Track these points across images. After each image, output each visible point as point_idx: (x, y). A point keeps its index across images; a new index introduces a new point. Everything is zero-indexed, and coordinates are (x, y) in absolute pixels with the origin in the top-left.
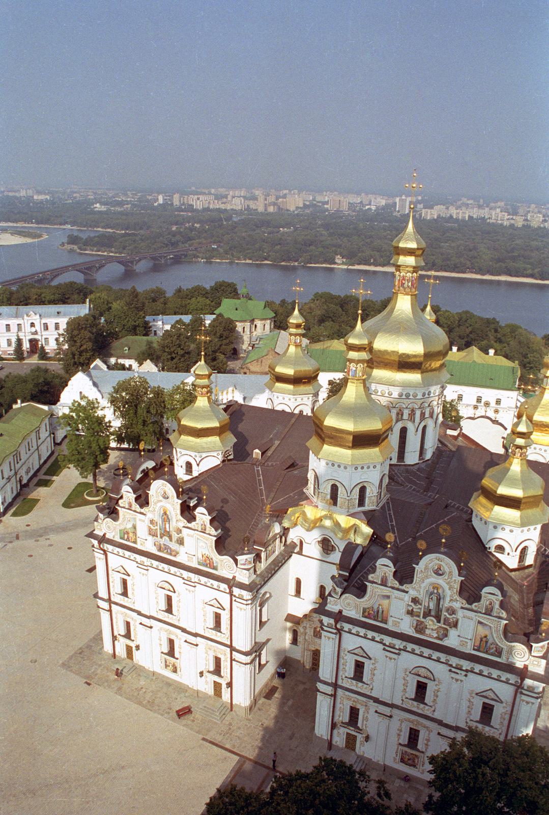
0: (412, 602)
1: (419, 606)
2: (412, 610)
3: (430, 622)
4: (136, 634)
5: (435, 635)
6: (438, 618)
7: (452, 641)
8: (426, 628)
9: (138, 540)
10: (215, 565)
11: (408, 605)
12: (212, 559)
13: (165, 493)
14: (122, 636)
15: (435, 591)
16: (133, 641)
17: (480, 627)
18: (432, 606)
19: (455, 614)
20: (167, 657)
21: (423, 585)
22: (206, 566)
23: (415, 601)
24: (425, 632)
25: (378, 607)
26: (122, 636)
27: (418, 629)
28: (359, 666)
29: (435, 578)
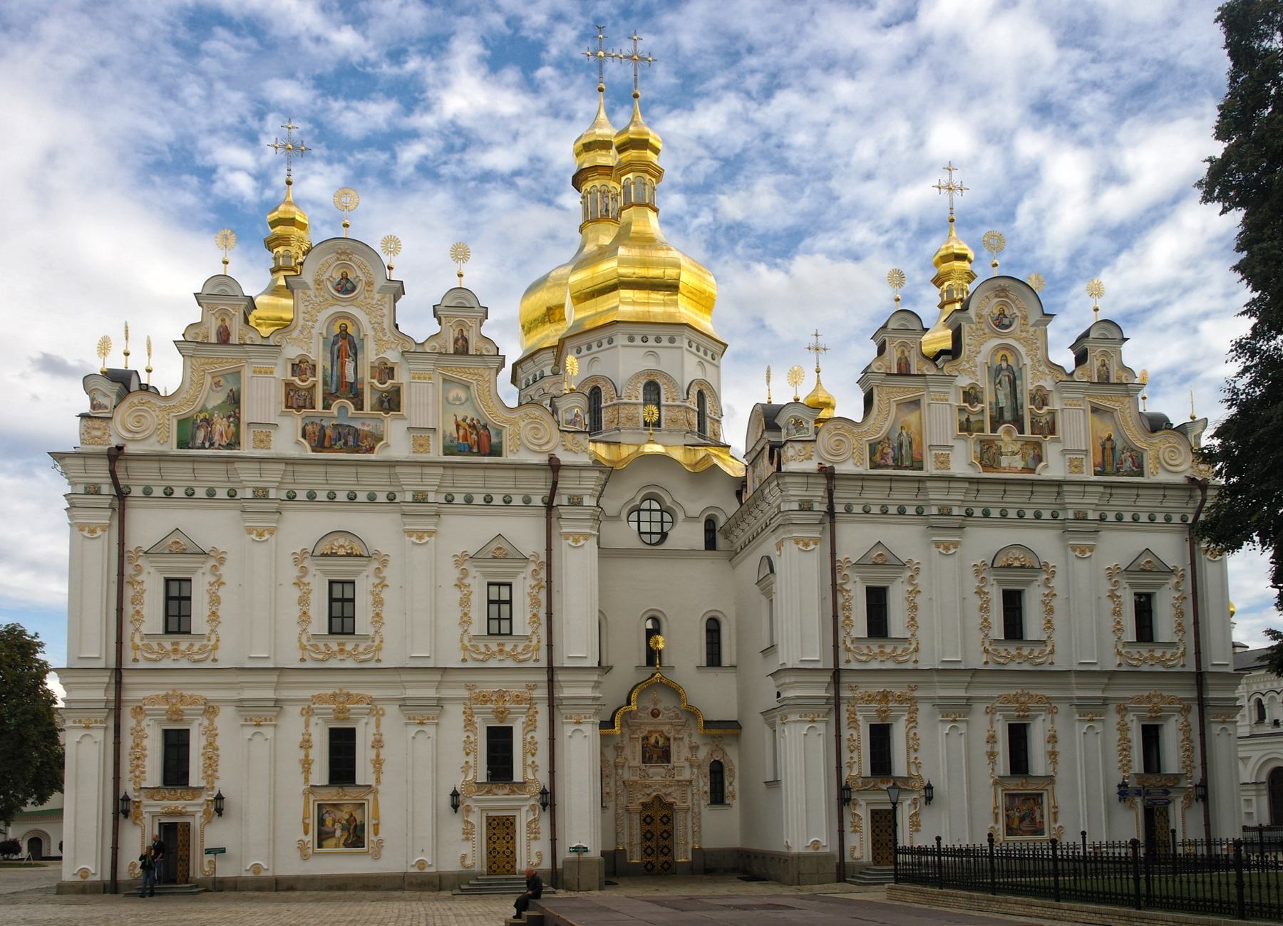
0: (964, 402)
1: (980, 406)
2: (968, 420)
3: (1006, 438)
4: (211, 761)
5: (1020, 465)
6: (1018, 422)
7: (1054, 467)
8: (1001, 454)
9: (246, 436)
10: (494, 440)
11: (961, 410)
12: (485, 427)
13: (345, 278)
14: (152, 792)
15: (1004, 365)
16: (199, 790)
17: (1096, 418)
18: (1004, 402)
19: (1047, 405)
20: (332, 795)
21: (980, 359)
22: (470, 453)
23: (971, 396)
24: (999, 463)
25: (900, 434)
26: (152, 792)
27: (985, 461)
28: (877, 600)
29: (999, 336)
